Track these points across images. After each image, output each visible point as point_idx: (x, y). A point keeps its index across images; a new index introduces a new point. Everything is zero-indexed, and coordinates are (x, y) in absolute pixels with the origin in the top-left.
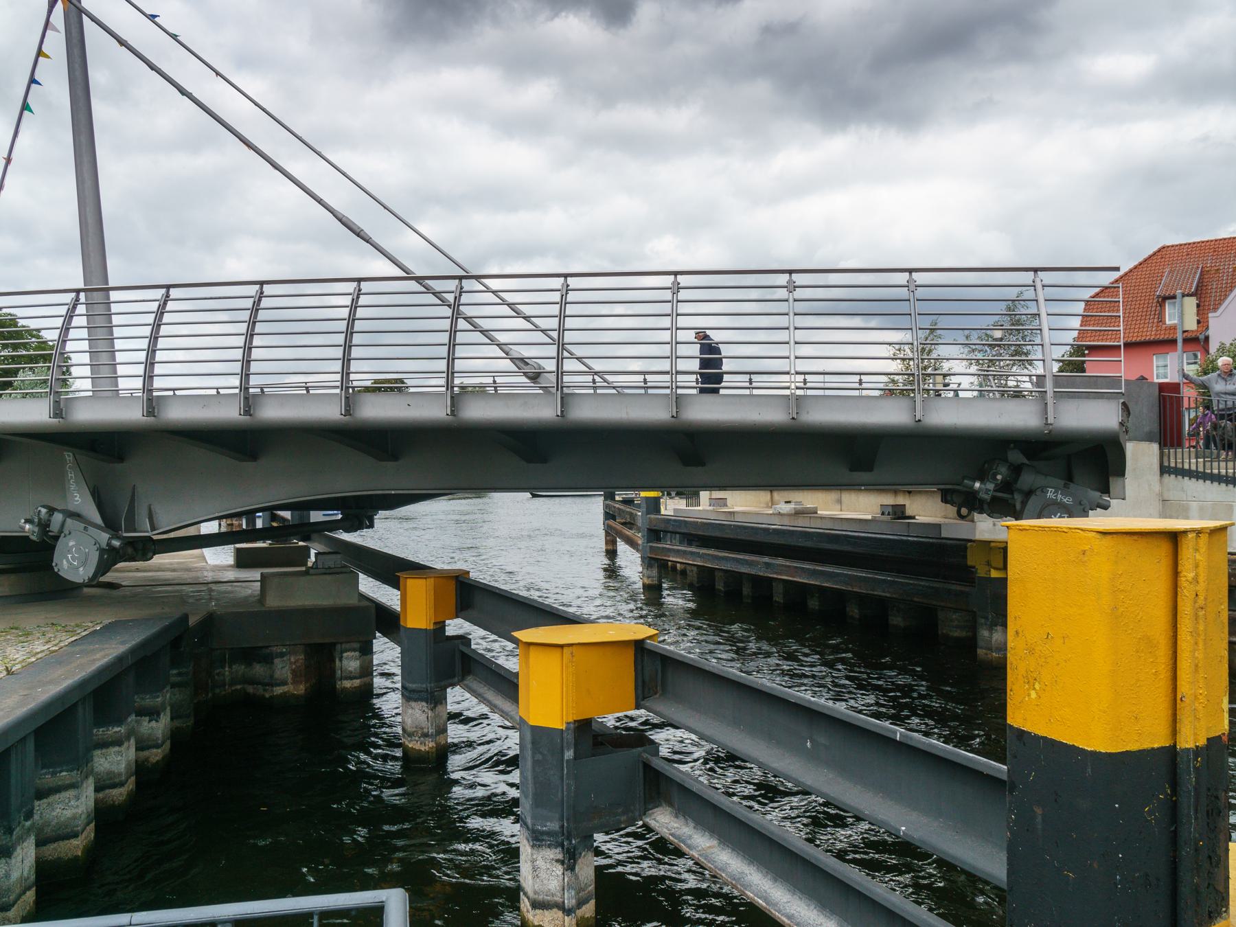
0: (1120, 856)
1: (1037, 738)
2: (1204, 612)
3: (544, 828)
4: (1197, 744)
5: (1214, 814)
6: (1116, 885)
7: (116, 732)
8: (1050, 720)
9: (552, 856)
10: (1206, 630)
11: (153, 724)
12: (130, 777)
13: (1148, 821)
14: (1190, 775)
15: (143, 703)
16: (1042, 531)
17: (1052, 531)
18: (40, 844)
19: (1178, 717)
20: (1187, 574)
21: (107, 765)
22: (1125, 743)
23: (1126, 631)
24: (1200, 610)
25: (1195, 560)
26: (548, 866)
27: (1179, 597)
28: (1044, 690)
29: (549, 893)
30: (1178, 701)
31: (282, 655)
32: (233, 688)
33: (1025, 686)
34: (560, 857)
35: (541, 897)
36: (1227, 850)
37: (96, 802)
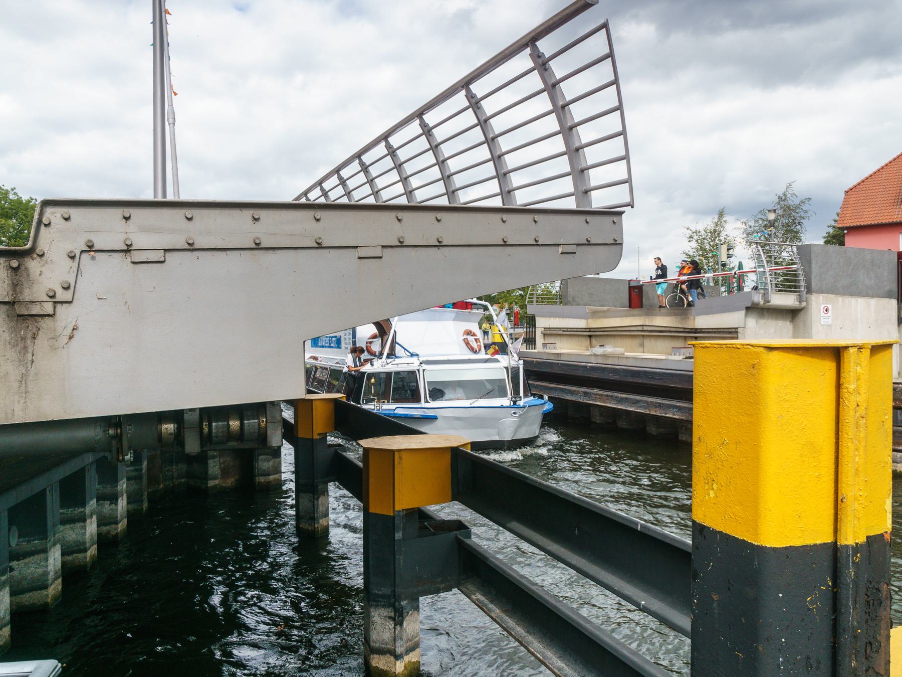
0: (783, 640)
1: (715, 532)
2: (865, 421)
3: (380, 592)
4: (857, 541)
5: (875, 604)
6: (778, 666)
7: (81, 512)
8: (725, 517)
9: (385, 614)
10: (866, 437)
11: (113, 506)
12: (92, 546)
13: (809, 609)
14: (848, 569)
15: (105, 491)
16: (721, 347)
17: (728, 347)
18: (12, 594)
19: (839, 517)
20: (850, 385)
21: (74, 536)
22: (789, 539)
23: (791, 438)
24: (861, 419)
25: (857, 373)
26: (383, 622)
27: (841, 407)
28: (721, 490)
29: (383, 641)
30: (839, 501)
31: (214, 457)
32: (179, 482)
33: (705, 487)
34: (392, 614)
35: (377, 645)
36: (888, 637)
37: (64, 564)
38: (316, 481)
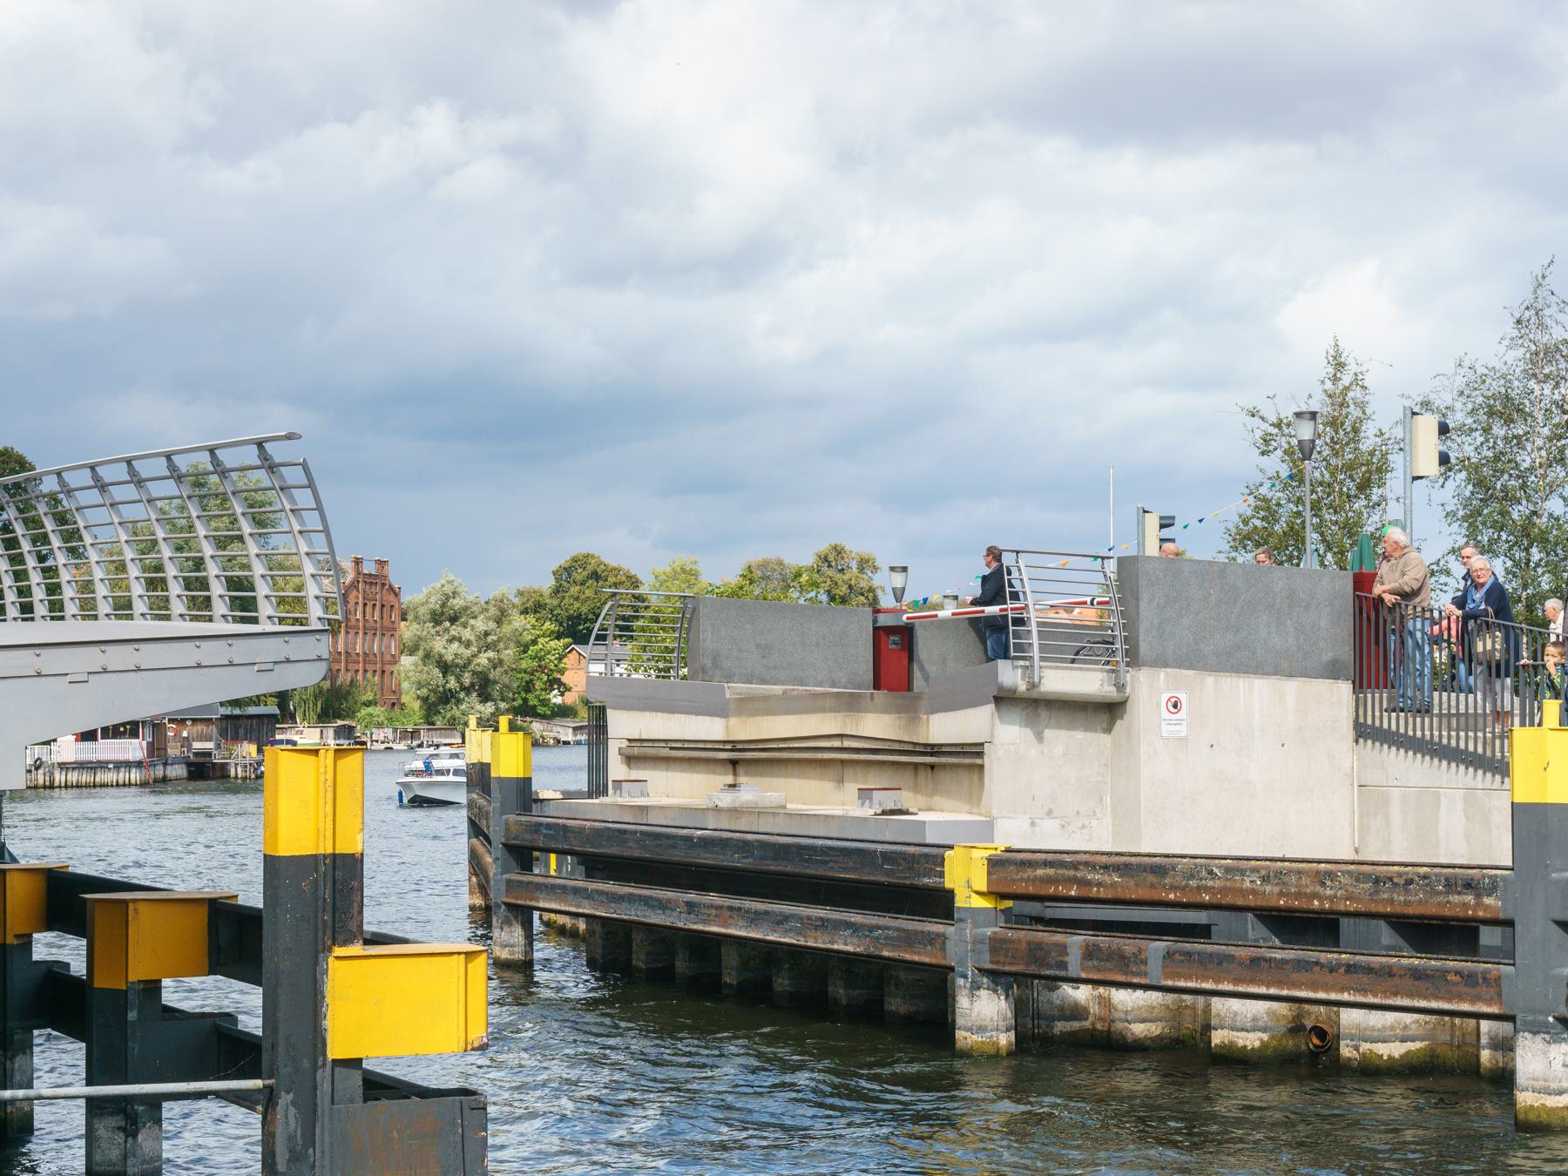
9: (114, 1124)
34: (122, 1124)
38: (9, 1024)
